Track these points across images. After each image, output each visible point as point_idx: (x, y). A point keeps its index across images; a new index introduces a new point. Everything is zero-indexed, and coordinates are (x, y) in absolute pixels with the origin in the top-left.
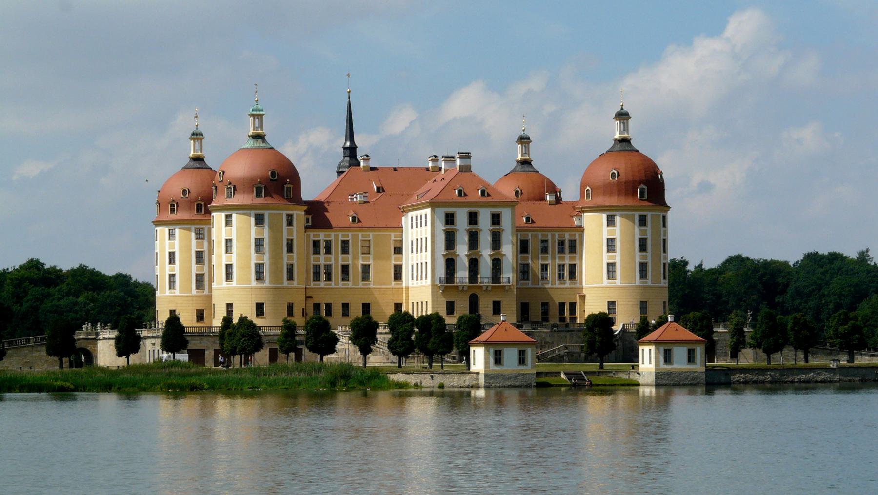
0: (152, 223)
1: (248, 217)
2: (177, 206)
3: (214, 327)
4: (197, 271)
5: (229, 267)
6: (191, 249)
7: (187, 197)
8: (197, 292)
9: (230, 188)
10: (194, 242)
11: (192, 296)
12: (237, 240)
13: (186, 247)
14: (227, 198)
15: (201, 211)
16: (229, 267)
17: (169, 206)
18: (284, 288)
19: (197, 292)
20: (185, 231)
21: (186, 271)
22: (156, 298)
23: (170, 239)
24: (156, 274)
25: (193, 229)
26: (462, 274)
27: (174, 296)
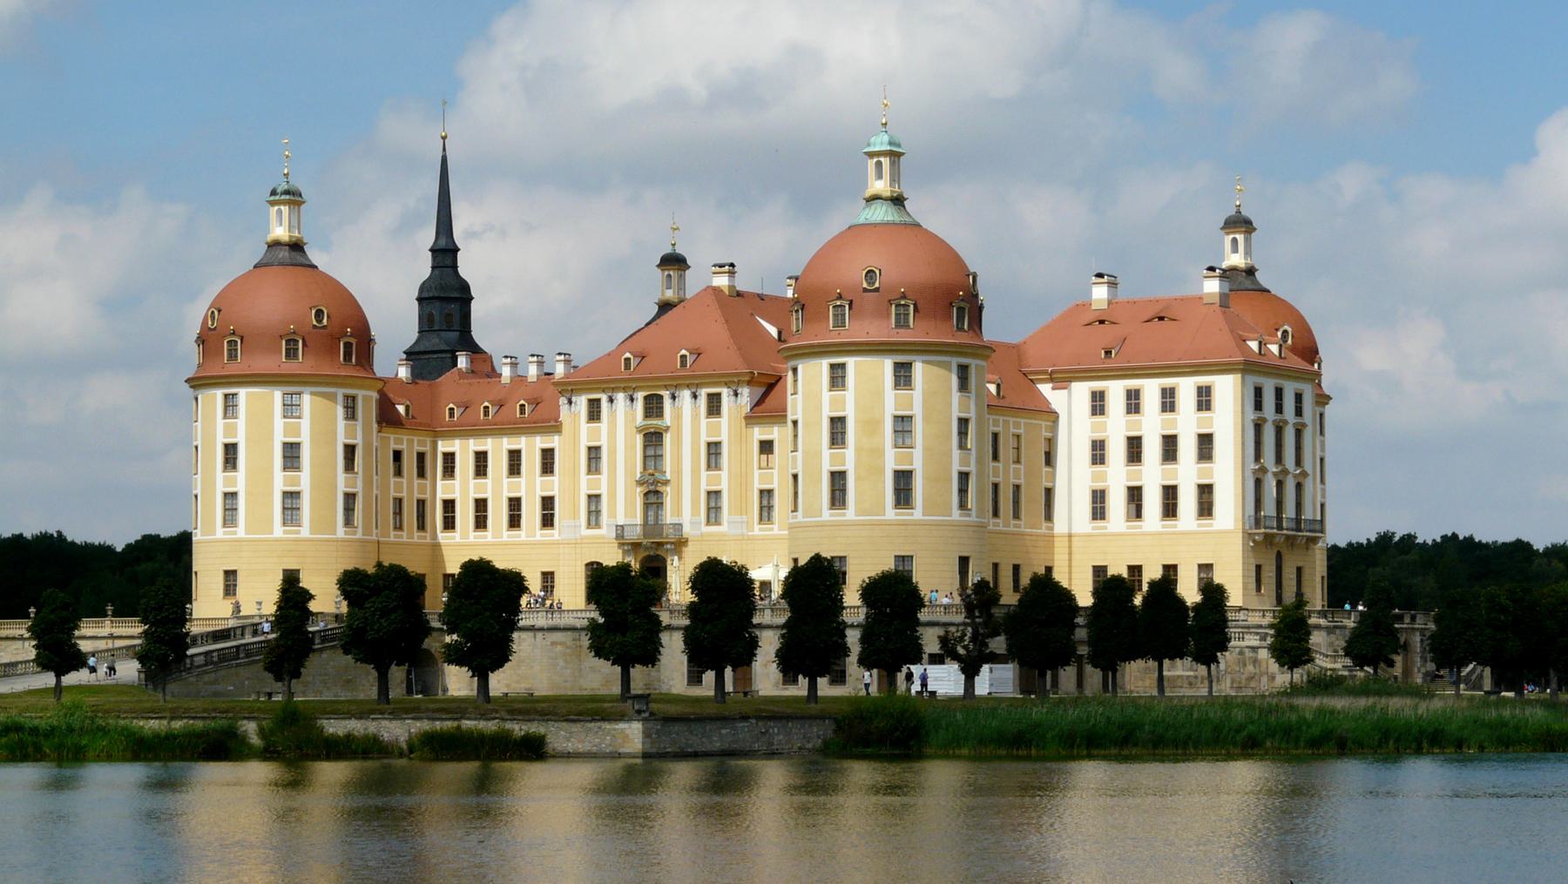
0: (187, 385)
1: (947, 372)
2: (304, 345)
3: (851, 607)
4: (284, 485)
5: (838, 478)
6: (336, 440)
7: (324, 327)
8: (346, 533)
9: (906, 306)
10: (341, 423)
11: (337, 540)
12: (926, 419)
13: (323, 435)
14: (897, 326)
15: (350, 360)
16: (838, 478)
17: (284, 342)
18: (822, 525)
19: (345, 531)
20: (325, 401)
21: (323, 484)
22: (194, 545)
23: (225, 417)
24: (194, 492)
25: (340, 398)
26: (1269, 509)
27: (295, 540)
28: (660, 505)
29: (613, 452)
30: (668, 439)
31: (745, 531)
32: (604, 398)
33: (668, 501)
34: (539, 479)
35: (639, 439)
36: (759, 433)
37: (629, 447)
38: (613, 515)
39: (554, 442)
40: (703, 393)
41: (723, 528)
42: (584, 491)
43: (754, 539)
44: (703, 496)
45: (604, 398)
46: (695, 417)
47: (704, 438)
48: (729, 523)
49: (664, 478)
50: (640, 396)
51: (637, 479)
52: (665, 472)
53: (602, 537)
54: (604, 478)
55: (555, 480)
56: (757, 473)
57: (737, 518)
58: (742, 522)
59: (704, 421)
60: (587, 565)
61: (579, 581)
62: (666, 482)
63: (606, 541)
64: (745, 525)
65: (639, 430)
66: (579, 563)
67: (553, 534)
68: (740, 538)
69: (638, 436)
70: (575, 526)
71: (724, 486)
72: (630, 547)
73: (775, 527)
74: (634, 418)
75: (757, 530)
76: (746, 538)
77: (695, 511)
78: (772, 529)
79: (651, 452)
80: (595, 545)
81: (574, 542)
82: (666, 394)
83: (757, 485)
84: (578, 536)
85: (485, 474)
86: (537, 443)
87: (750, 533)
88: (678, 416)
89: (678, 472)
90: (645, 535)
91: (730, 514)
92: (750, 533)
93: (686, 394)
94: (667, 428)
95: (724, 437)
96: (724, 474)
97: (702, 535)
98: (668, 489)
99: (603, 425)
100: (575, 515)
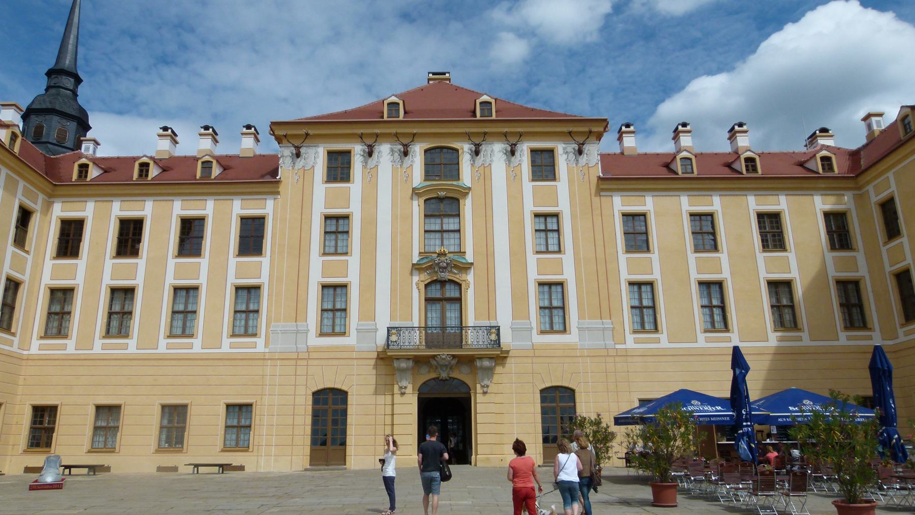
28: (459, 300)
29: (370, 222)
30: (467, 206)
31: (610, 343)
32: (358, 149)
33: (470, 298)
34: (233, 261)
35: (417, 208)
36: (619, 204)
37: (400, 219)
38: (369, 313)
39: (267, 207)
40: (525, 148)
41: (572, 338)
42: (316, 276)
43: (626, 355)
44: (533, 288)
45: (358, 149)
46: (513, 178)
47: (529, 207)
48: (580, 329)
49: (464, 261)
50: (418, 150)
51: (415, 262)
52: (465, 252)
53: (351, 349)
54: (354, 261)
55: (264, 261)
56: (623, 258)
57: (597, 323)
58: (604, 329)
59: (528, 186)
60: (316, 394)
61: (299, 420)
62: (467, 267)
63: (354, 355)
64: (608, 334)
65: (416, 193)
66: (301, 390)
67: (259, 344)
68: (604, 353)
69: (415, 203)
70: (297, 332)
71: (568, 275)
72: (410, 363)
73: (663, 337)
74: (409, 177)
75: (631, 341)
76: (612, 353)
77: (519, 309)
78: (658, 341)
79: (435, 224)
80: (335, 362)
81: (295, 356)
82: (465, 148)
83: (625, 276)
84: (302, 347)
85: (135, 253)
86: (239, 208)
87: (618, 346)
88: (485, 176)
89: (489, 255)
90: (430, 343)
91: (581, 317)
92: (618, 346)
93: (496, 150)
94: (465, 192)
95: (564, 206)
96: (568, 259)
97: (533, 348)
98: (470, 277)
99: (355, 187)
100: (299, 314)
